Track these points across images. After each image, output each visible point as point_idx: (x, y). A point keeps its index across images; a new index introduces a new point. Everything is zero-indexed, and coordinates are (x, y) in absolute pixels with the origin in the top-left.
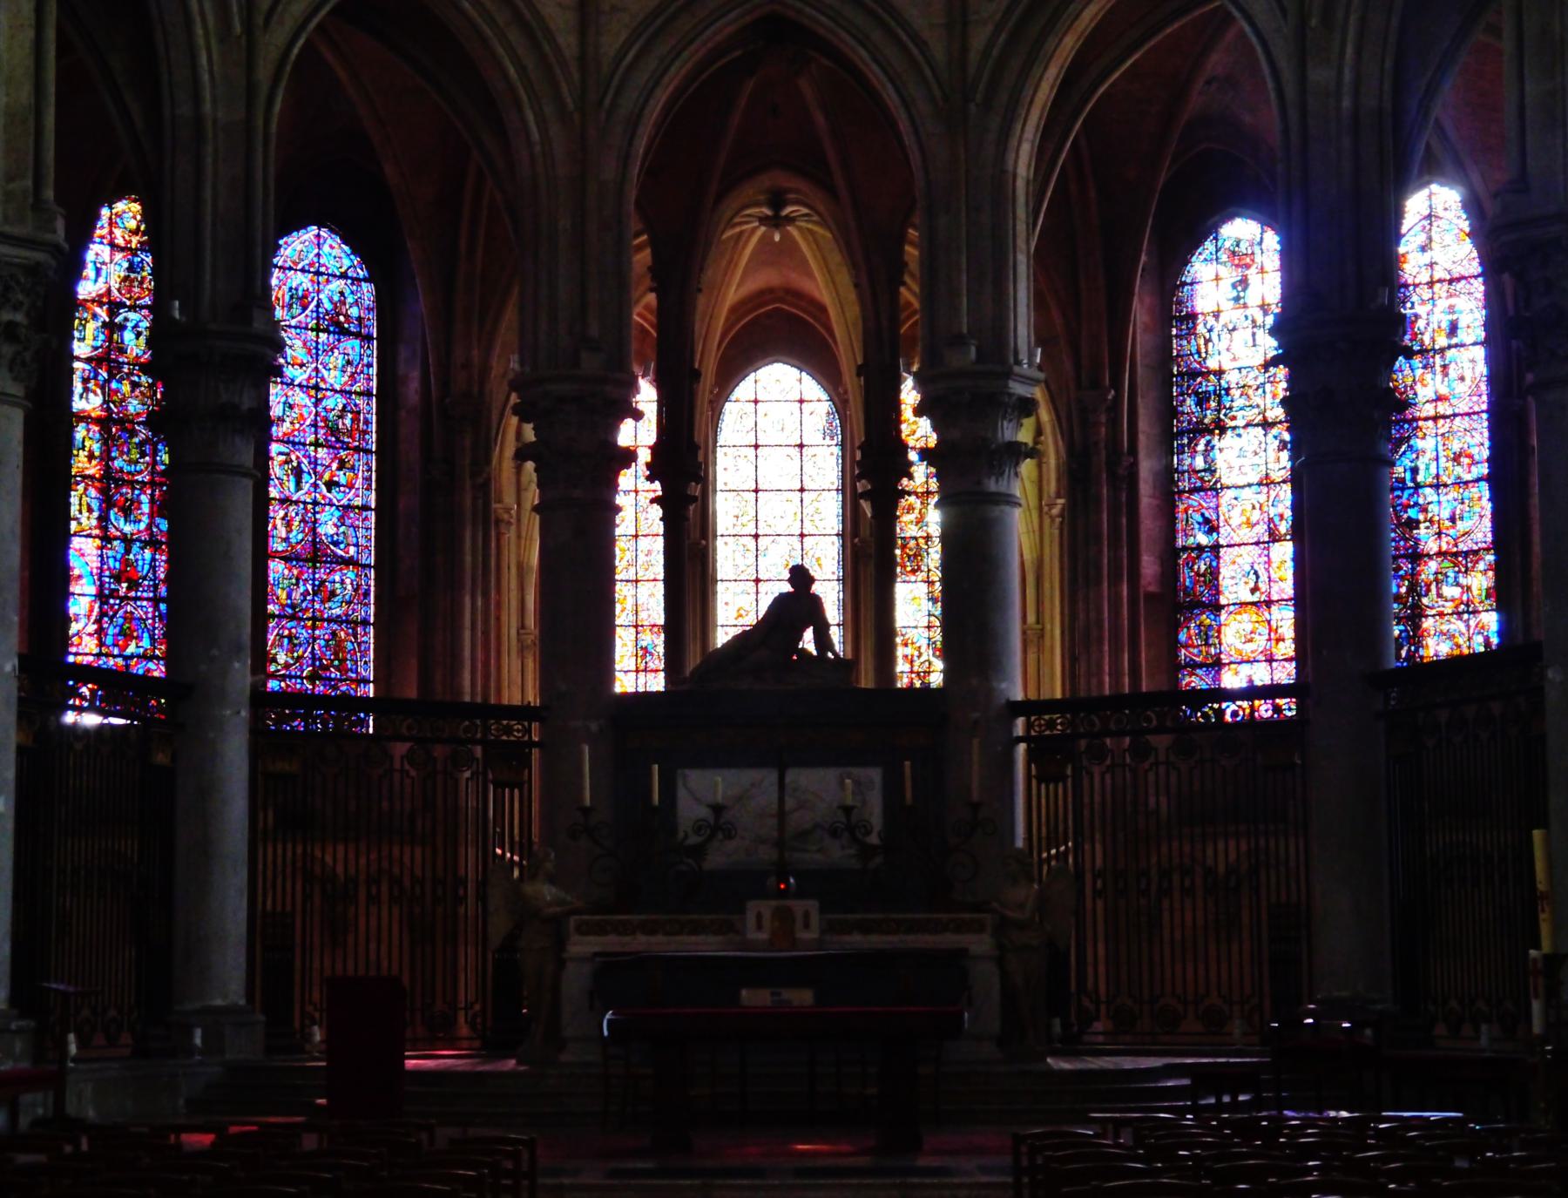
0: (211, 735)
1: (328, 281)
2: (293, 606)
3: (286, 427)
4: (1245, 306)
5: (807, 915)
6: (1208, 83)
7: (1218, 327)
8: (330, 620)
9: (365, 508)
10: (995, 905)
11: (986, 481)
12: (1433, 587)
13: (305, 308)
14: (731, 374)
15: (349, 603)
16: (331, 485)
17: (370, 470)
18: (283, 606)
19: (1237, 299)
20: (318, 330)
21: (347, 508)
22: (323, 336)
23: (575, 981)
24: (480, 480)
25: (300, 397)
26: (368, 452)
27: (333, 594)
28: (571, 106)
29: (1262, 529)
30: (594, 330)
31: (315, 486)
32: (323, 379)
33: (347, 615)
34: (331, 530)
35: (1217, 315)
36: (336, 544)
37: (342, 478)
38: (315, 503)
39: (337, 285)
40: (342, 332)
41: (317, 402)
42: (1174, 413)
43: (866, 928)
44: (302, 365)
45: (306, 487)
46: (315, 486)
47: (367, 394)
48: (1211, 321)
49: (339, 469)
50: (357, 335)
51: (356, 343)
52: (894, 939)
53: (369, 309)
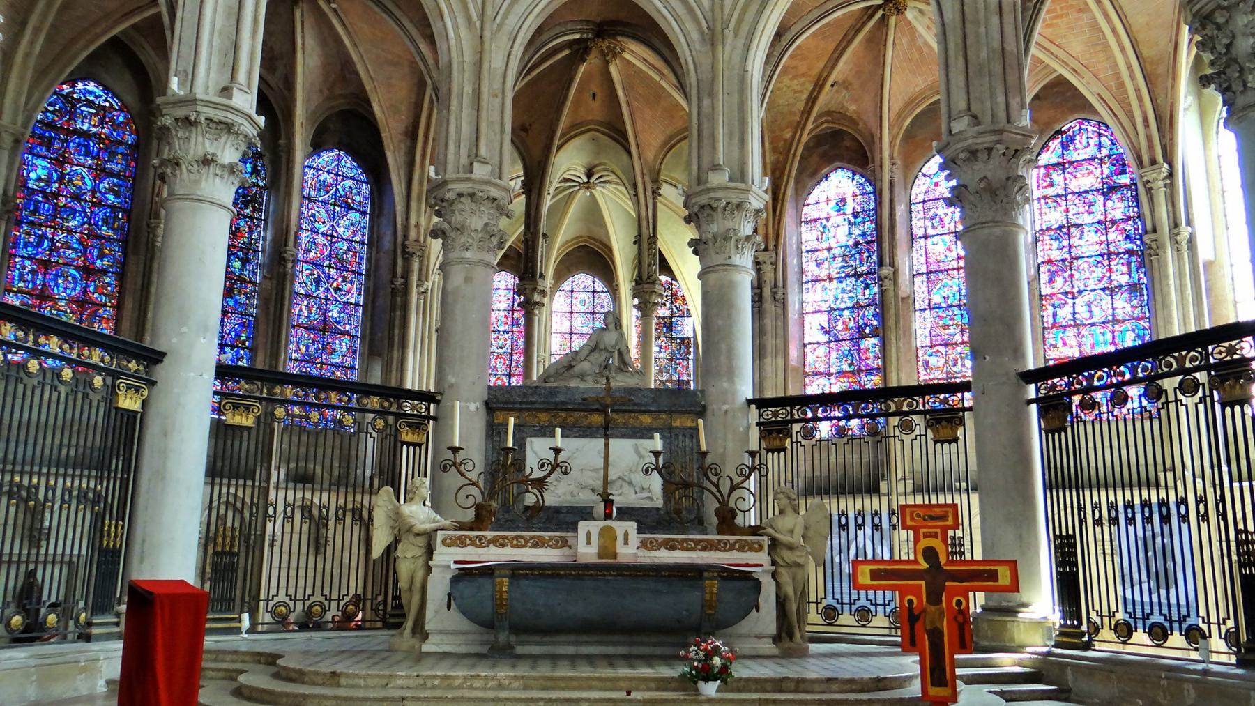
0: (176, 390)
1: (343, 180)
2: (309, 355)
3: (312, 255)
4: (844, 214)
5: (626, 535)
6: (832, 86)
7: (829, 226)
8: (332, 365)
9: (357, 304)
10: (770, 530)
11: (733, 256)
12: (959, 361)
13: (328, 192)
14: (560, 276)
15: (344, 356)
16: (337, 289)
17: (361, 284)
18: (303, 355)
19: (838, 211)
20: (335, 205)
21: (347, 303)
22: (338, 209)
23: (438, 587)
24: (422, 290)
25: (320, 239)
26: (361, 274)
27: (334, 350)
28: (475, 18)
29: (854, 332)
30: (483, 152)
31: (328, 289)
32: (336, 232)
33: (342, 363)
34: (336, 315)
35: (827, 219)
36: (338, 323)
37: (346, 287)
38: (327, 299)
39: (348, 183)
40: (349, 208)
41: (332, 244)
42: (802, 271)
43: (670, 545)
44: (324, 223)
45: (322, 289)
46: (328, 289)
47: (362, 243)
48: (824, 222)
49: (343, 281)
50: (358, 211)
51: (357, 215)
52: (693, 554)
53: (367, 198)
